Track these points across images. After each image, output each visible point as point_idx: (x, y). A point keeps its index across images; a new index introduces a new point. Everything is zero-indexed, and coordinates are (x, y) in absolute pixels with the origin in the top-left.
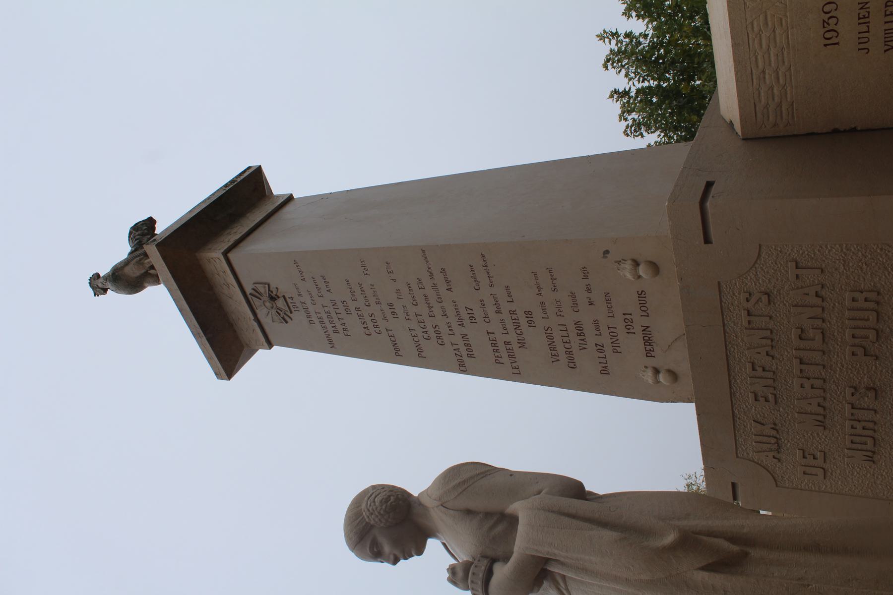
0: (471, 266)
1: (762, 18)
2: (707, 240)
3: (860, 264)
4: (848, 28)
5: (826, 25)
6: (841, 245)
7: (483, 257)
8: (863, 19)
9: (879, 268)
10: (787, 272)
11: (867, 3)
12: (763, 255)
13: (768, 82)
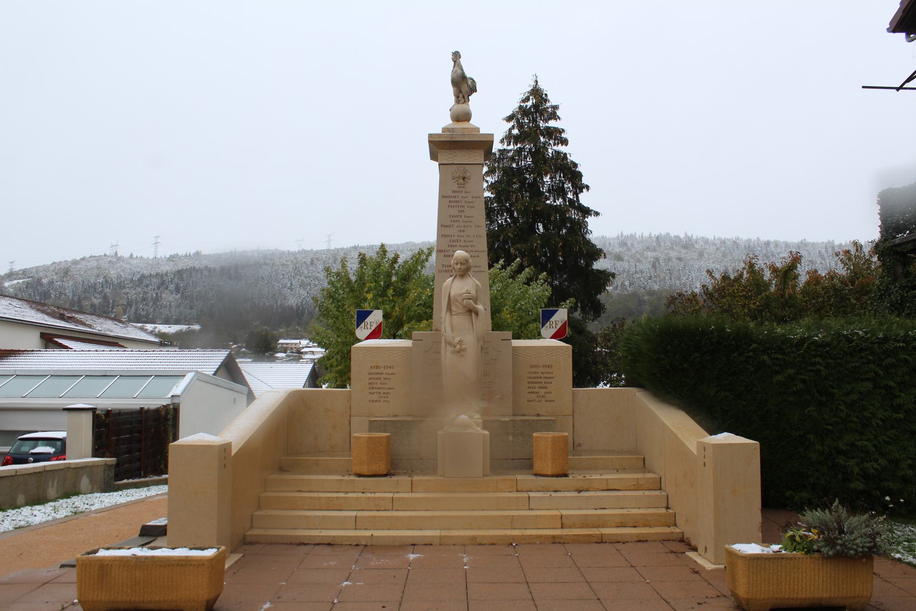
2: (502, 340)
4: (534, 370)
7: (484, 272)
8: (535, 373)
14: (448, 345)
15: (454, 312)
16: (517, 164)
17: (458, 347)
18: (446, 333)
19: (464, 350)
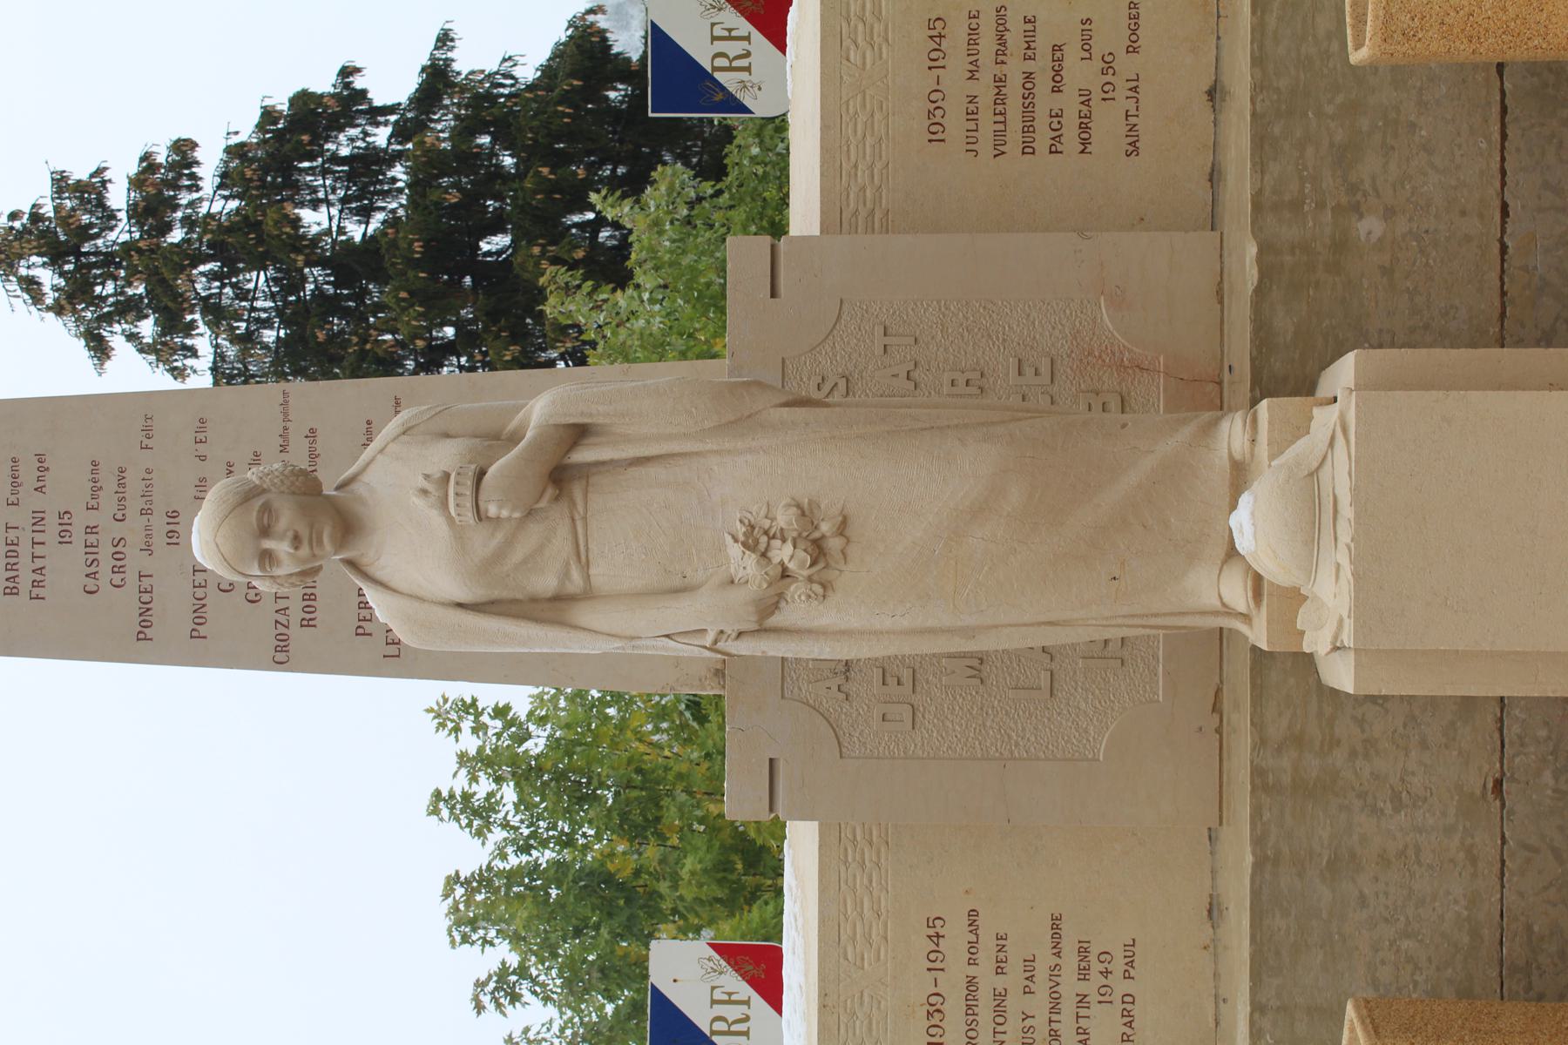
0: (369, 423)
1: (859, 98)
2: (774, 294)
3: (961, 330)
4: (955, 124)
5: (931, 116)
6: (939, 302)
8: (972, 115)
9: (983, 337)
10: (873, 342)
11: (975, 97)
12: (844, 317)
13: (860, 180)
14: (775, 620)
15: (565, 575)
16: (267, 323)
17: (783, 553)
18: (704, 631)
19: (806, 513)
